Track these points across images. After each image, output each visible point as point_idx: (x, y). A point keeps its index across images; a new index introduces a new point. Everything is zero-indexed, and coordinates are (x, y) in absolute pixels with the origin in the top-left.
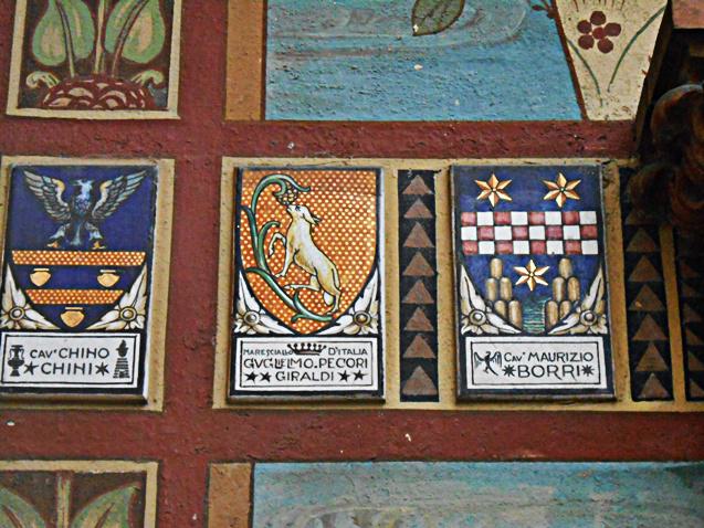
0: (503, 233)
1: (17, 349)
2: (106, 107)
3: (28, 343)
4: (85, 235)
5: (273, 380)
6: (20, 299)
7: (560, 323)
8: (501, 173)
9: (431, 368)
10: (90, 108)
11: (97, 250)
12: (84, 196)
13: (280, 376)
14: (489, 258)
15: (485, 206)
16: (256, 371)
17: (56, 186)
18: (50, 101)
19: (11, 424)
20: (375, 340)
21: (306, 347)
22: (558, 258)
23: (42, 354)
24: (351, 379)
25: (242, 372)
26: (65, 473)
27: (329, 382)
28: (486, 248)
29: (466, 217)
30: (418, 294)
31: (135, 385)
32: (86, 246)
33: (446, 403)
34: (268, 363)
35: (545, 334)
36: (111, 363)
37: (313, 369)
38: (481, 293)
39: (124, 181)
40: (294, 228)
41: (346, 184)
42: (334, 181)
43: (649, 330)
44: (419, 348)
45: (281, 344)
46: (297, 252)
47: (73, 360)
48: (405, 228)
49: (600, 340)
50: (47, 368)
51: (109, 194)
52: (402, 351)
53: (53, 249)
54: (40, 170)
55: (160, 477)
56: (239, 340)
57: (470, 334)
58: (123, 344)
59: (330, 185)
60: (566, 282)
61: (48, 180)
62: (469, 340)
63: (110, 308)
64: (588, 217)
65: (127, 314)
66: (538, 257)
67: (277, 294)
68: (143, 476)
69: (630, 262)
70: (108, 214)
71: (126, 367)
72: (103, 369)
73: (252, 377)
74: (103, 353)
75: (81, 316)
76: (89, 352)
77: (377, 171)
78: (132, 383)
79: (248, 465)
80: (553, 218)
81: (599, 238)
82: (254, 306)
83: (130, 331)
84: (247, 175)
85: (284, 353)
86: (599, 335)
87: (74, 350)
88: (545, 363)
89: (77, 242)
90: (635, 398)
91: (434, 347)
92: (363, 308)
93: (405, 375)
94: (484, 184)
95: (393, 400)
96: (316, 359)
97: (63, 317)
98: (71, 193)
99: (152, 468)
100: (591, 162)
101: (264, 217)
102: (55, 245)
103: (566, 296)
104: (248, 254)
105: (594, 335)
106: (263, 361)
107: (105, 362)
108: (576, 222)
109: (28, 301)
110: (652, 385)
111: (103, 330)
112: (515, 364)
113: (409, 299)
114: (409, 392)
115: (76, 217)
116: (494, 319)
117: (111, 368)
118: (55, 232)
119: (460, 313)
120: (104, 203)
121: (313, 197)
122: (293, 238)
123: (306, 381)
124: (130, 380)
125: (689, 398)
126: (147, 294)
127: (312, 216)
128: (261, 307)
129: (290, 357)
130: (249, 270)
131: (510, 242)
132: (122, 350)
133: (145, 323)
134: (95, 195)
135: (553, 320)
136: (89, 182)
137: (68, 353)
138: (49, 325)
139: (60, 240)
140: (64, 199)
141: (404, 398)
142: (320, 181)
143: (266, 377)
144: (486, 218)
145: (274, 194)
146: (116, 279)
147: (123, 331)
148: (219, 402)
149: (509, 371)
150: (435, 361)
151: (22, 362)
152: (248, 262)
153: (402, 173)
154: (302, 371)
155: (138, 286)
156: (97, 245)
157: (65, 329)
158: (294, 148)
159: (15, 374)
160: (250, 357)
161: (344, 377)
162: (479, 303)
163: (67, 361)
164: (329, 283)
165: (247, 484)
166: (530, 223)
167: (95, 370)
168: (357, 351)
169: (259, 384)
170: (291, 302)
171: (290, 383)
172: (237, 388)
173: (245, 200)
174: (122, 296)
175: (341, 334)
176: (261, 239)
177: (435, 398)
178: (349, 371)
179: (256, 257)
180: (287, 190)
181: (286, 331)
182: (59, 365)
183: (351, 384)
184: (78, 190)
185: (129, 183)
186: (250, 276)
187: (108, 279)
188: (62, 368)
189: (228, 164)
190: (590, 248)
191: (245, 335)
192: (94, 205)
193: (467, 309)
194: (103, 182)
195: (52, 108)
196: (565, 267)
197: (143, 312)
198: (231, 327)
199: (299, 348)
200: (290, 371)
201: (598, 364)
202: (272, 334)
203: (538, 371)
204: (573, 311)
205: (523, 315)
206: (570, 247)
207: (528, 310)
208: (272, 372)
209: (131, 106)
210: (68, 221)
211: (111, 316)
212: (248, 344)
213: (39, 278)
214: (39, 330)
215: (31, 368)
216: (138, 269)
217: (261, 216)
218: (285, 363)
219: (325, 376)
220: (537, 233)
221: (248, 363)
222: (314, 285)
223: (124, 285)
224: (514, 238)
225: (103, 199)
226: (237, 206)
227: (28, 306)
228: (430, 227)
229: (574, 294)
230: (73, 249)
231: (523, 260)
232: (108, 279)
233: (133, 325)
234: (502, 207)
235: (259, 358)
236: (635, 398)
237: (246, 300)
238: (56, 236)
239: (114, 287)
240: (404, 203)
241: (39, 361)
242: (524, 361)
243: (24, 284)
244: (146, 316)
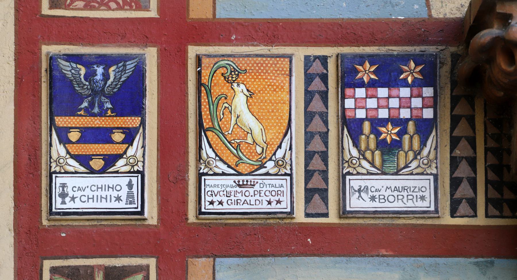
0: (372, 103)
1: (64, 186)
2: (109, 9)
3: (71, 181)
4: (101, 105)
5: (225, 205)
6: (62, 151)
7: (406, 166)
8: (372, 59)
9: (324, 193)
10: (98, 9)
11: (110, 116)
12: (99, 77)
13: (229, 202)
14: (362, 121)
15: (361, 85)
16: (215, 199)
17: (80, 69)
18: (70, 5)
19: (64, 235)
20: (288, 178)
21: (245, 183)
22: (407, 120)
23: (79, 189)
24: (274, 204)
25: (206, 199)
26: (99, 267)
27: (260, 206)
28: (361, 114)
29: (349, 91)
30: (317, 145)
31: (139, 209)
32: (102, 114)
33: (333, 219)
34: (221, 193)
35: (396, 174)
36: (124, 193)
37: (250, 198)
38: (356, 144)
39: (125, 66)
40: (236, 100)
41: (270, 67)
42: (262, 65)
43: (463, 171)
44: (316, 182)
45: (229, 181)
46: (238, 117)
47: (99, 193)
48: (309, 96)
49: (432, 178)
50: (83, 199)
51: (115, 75)
52: (306, 183)
53: (81, 115)
54: (71, 58)
55: (158, 268)
56: (203, 178)
57: (349, 173)
58: (130, 181)
59: (260, 69)
60: (411, 138)
61: (74, 65)
62: (348, 177)
63: (120, 156)
64: (428, 92)
65: (132, 161)
66: (396, 121)
67: (226, 146)
68: (147, 268)
69: (455, 121)
70: (115, 90)
71: (133, 197)
72: (118, 199)
73: (212, 203)
74: (118, 188)
75: (103, 162)
76: (109, 187)
77: (290, 57)
78: (137, 208)
79: (212, 259)
80: (405, 92)
81: (435, 107)
82: (213, 155)
83: (134, 172)
84: (205, 61)
85: (232, 187)
86: (431, 174)
87: (100, 186)
88: (396, 193)
89: (96, 110)
90: (452, 216)
91: (326, 180)
92: (282, 156)
93: (308, 200)
94: (360, 68)
95: (300, 217)
96: (251, 190)
97: (91, 163)
98: (90, 75)
99: (152, 262)
100: (431, 49)
101: (216, 91)
102: (82, 112)
103: (411, 148)
104: (207, 118)
105: (427, 174)
106: (219, 192)
107: (120, 193)
108: (420, 95)
109: (68, 152)
110: (464, 207)
111: (117, 172)
112: (377, 194)
113: (310, 148)
114: (309, 211)
115: (95, 93)
116: (365, 163)
117: (124, 198)
118: (82, 103)
119: (343, 159)
120: (112, 83)
121: (248, 77)
122: (236, 107)
123: (245, 206)
124: (136, 206)
125: (487, 216)
126: (144, 147)
127: (248, 90)
128: (217, 155)
129: (235, 189)
130: (208, 129)
131: (377, 109)
132: (130, 185)
133: (143, 166)
134: (106, 76)
135: (402, 165)
136: (102, 67)
137: (95, 188)
138: (82, 169)
139: (86, 109)
140: (86, 79)
141: (307, 215)
142: (253, 66)
143: (221, 203)
144: (360, 92)
145: (222, 74)
146: (123, 136)
147: (129, 172)
148: (192, 218)
149: (373, 198)
150: (326, 190)
151: (67, 195)
152: (208, 124)
153: (307, 58)
154: (243, 198)
155: (138, 140)
156: (109, 112)
157: (92, 171)
158: (236, 39)
159: (63, 203)
160: (211, 189)
161: (270, 203)
162: (355, 152)
163: (95, 194)
164: (259, 139)
165: (211, 272)
166: (390, 97)
167: (113, 199)
168: (277, 186)
169: (217, 207)
170: (235, 152)
171: (236, 207)
172: (203, 210)
173: (204, 80)
174: (127, 148)
175: (267, 174)
176: (215, 106)
177: (326, 215)
178: (272, 199)
179: (212, 120)
180: (231, 72)
181: (233, 172)
182: (91, 196)
183: (274, 208)
184: (95, 73)
185: (128, 67)
186: (209, 133)
187: (118, 137)
188: (93, 198)
189: (193, 51)
190: (428, 114)
191: (207, 174)
192: (106, 83)
193: (347, 157)
194: (110, 67)
195: (72, 9)
196: (411, 127)
197: (142, 159)
198: (198, 169)
199: (241, 183)
200: (236, 198)
201: (429, 194)
202: (223, 174)
203: (391, 199)
204: (415, 158)
205: (383, 161)
206: (415, 112)
207: (386, 157)
208: (225, 199)
209: (126, 7)
210: (90, 95)
211: (121, 162)
212: (210, 181)
213: (74, 136)
214: (76, 173)
215: (73, 199)
216: (136, 130)
217: (215, 91)
218: (233, 194)
219: (258, 202)
220: (394, 103)
221: (209, 193)
222: (250, 140)
223: (129, 140)
224: (379, 107)
225: (112, 79)
226: (199, 84)
227: (68, 156)
228: (324, 96)
229: (416, 145)
230: (94, 115)
231: (384, 122)
232: (118, 137)
233: (136, 168)
234: (373, 85)
235: (216, 190)
236: (452, 216)
237: (207, 151)
238: (83, 106)
239: (123, 142)
240: (309, 79)
241: (78, 194)
242: (383, 192)
243: (64, 140)
244: (144, 162)
